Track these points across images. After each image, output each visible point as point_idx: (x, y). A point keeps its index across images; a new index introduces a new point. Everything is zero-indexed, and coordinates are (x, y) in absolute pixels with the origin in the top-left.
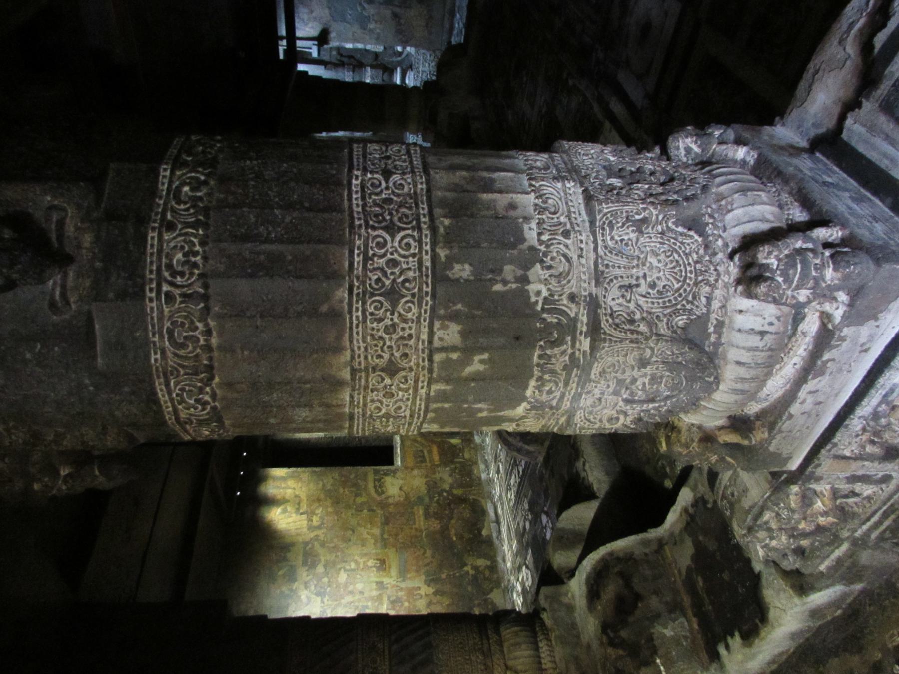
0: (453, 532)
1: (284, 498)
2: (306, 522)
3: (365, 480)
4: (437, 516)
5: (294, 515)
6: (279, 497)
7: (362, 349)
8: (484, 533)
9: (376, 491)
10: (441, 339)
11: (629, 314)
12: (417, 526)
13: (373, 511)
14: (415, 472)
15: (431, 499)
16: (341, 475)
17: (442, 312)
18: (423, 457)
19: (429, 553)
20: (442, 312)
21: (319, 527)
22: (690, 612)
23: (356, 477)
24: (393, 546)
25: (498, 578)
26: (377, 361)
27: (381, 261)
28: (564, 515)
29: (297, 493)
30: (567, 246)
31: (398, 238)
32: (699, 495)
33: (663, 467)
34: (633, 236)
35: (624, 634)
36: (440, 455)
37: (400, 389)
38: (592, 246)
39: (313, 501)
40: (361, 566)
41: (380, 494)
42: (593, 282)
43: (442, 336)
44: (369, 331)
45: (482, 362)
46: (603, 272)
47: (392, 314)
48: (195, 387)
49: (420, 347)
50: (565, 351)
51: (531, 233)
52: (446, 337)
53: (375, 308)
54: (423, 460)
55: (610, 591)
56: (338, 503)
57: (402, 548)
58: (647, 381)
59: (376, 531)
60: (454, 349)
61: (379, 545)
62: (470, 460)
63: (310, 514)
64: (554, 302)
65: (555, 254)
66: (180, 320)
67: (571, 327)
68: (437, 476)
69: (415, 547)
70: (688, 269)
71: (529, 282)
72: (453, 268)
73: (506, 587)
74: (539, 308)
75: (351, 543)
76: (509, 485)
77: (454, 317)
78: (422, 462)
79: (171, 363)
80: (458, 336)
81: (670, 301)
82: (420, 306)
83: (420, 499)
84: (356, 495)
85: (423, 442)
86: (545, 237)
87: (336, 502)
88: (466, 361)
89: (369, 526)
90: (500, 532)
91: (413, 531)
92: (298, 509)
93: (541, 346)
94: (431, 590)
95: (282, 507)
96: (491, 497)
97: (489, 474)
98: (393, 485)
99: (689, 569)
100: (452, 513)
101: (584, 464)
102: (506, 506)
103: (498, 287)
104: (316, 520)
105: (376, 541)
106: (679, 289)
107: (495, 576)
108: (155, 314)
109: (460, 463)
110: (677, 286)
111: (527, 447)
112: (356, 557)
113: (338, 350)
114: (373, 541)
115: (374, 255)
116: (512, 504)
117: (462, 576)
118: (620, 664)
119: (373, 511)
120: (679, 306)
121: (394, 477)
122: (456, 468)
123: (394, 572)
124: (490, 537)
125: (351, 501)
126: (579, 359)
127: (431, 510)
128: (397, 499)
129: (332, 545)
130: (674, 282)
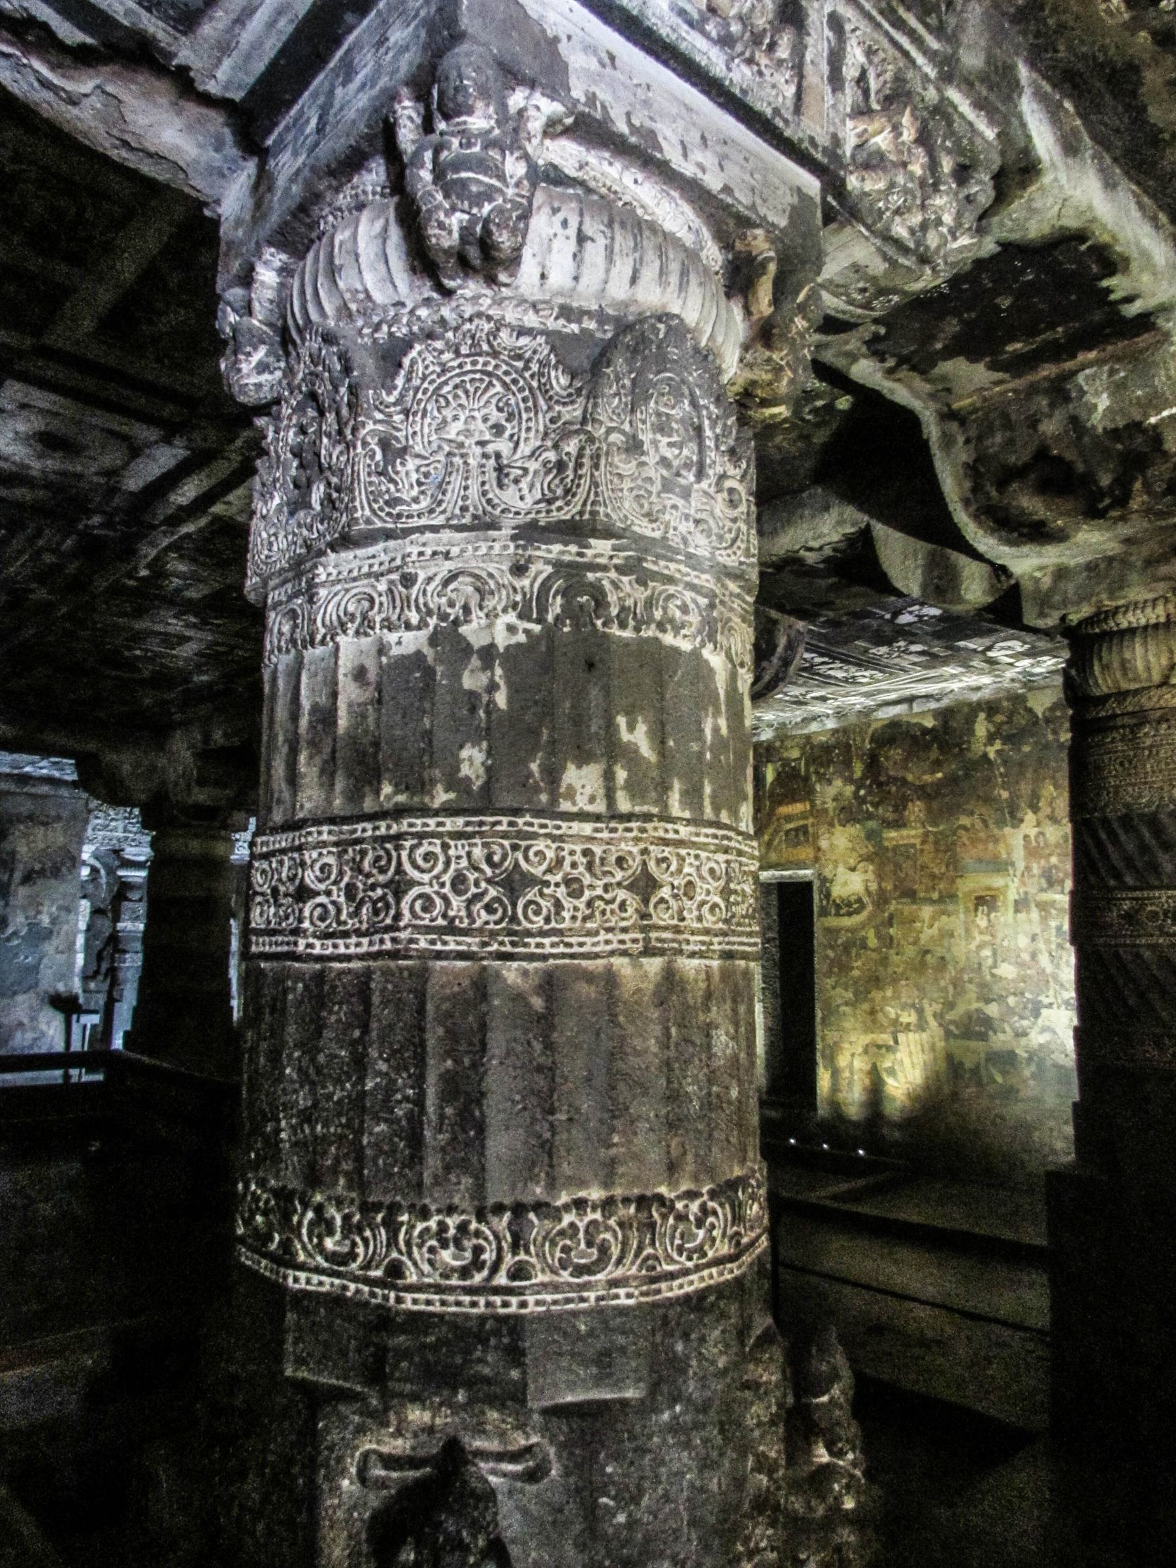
0: (927, 778)
4: (900, 805)
5: (899, 1055)
6: (867, 1082)
7: (610, 936)
8: (929, 723)
9: (857, 912)
10: (592, 799)
11: (549, 471)
12: (917, 841)
14: (824, 844)
15: (870, 816)
16: (829, 973)
17: (544, 798)
18: (797, 830)
19: (965, 821)
20: (544, 798)
21: (920, 1012)
22: (1069, 365)
23: (832, 947)
24: (953, 882)
26: (630, 910)
27: (455, 904)
28: (899, 585)
30: (430, 579)
31: (414, 874)
32: (864, 349)
33: (815, 411)
34: (411, 463)
35: (1105, 480)
36: (794, 800)
37: (679, 871)
38: (429, 536)
39: (874, 1021)
40: (987, 938)
41: (863, 906)
42: (493, 533)
43: (586, 798)
44: (578, 923)
45: (631, 728)
46: (475, 517)
47: (547, 884)
48: (675, 1228)
49: (605, 835)
50: (613, 582)
51: (407, 642)
52: (588, 790)
53: (537, 913)
54: (804, 830)
55: (1031, 504)
56: (877, 979)
57: (955, 867)
58: (665, 440)
59: (927, 911)
60: (609, 776)
61: (950, 908)
62: (803, 749)
63: (897, 1027)
64: (527, 602)
65: (444, 600)
66: (558, 1254)
67: (571, 575)
68: (830, 805)
70: (468, 367)
71: (492, 646)
72: (468, 778)
73: (1025, 685)
74: (537, 628)
75: (948, 957)
76: (846, 680)
77: (553, 775)
78: (806, 833)
79: (634, 1270)
80: (586, 770)
81: (524, 400)
82: (534, 836)
83: (871, 835)
84: (864, 946)
85: (770, 830)
86: (414, 618)
87: (876, 981)
88: (630, 755)
90: (928, 697)
92: (889, 1048)
93: (604, 624)
94: (1030, 817)
96: (867, 713)
99: (993, 367)
100: (896, 779)
101: (810, 549)
102: (882, 686)
103: (501, 699)
106: (504, 384)
108: (549, 1298)
110: (498, 388)
111: (780, 649)
112: (973, 947)
113: (610, 979)
114: (944, 918)
115: (445, 916)
116: (879, 675)
117: (1005, 763)
118: (1159, 488)
119: (891, 917)
120: (535, 384)
123: (998, 881)
124: (936, 714)
125: (874, 955)
126: (627, 558)
127: (890, 816)
128: (871, 876)
129: (951, 989)
130: (492, 391)
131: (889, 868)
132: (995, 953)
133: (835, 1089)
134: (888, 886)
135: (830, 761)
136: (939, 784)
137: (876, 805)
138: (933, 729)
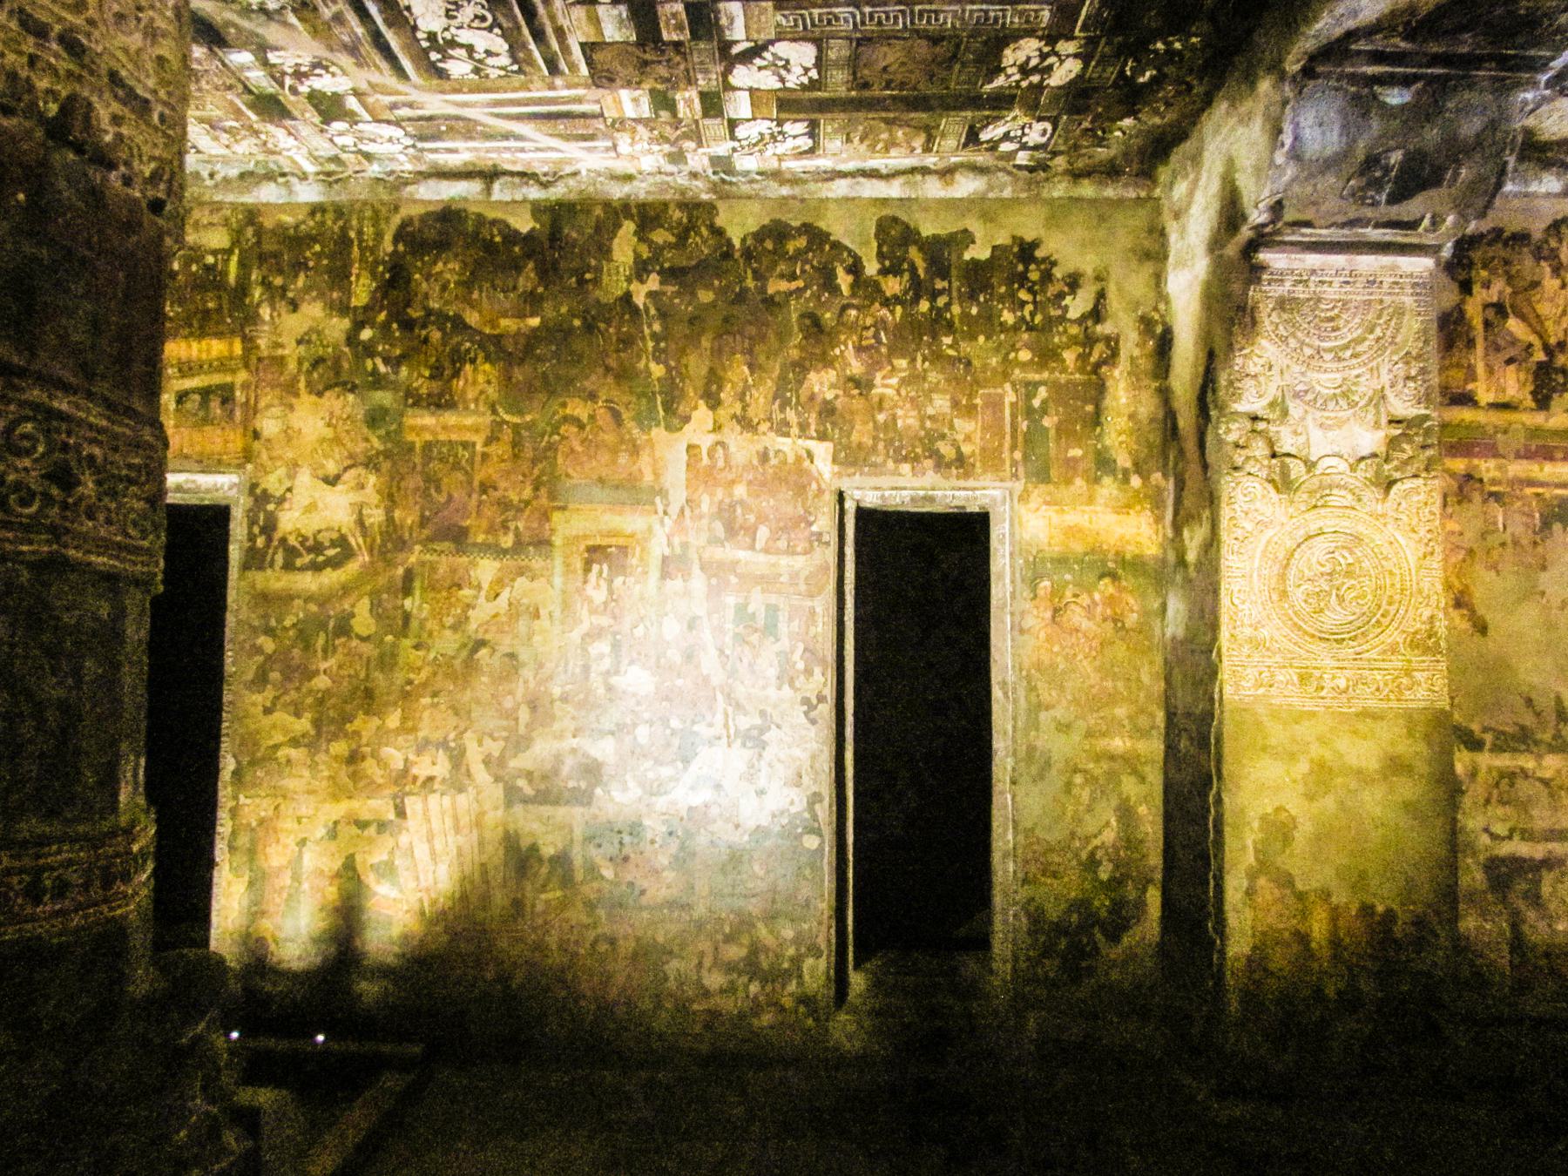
0: (508, 324)
1: (338, 875)
2: (433, 799)
3: (287, 598)
4: (448, 367)
5: (404, 839)
6: (332, 893)
8: (524, 223)
9: (335, 563)
12: (479, 440)
14: (269, 425)
15: (378, 382)
16: (261, 680)
18: (206, 393)
19: (579, 409)
21: (458, 759)
23: (269, 631)
24: (545, 516)
25: (682, 206)
29: (321, 832)
36: (202, 334)
39: (354, 776)
40: (604, 621)
41: (347, 553)
56: (369, 694)
57: (549, 489)
59: (486, 569)
61: (537, 563)
68: (291, 351)
69: (551, 447)
73: (714, 188)
75: (524, 656)
83: (375, 419)
84: (344, 628)
87: (368, 699)
89: (466, 592)
90: (525, 176)
91: (496, 450)
92: (382, 826)
95: (370, 879)
97: (304, 177)
98: (311, 508)
100: (441, 318)
104: (437, 765)
105: (521, 572)
107: (677, 214)
112: (576, 635)
114: (521, 582)
117: (663, 315)
119: (409, 576)
121: (281, 501)
122: (266, 284)
123: (631, 522)
124: (537, 209)
125: (367, 649)
127: (423, 385)
128: (371, 494)
129: (524, 714)
131: (414, 481)
132: (616, 646)
133: (256, 912)
134: (407, 517)
135: (299, 266)
136: (533, 339)
138: (530, 237)
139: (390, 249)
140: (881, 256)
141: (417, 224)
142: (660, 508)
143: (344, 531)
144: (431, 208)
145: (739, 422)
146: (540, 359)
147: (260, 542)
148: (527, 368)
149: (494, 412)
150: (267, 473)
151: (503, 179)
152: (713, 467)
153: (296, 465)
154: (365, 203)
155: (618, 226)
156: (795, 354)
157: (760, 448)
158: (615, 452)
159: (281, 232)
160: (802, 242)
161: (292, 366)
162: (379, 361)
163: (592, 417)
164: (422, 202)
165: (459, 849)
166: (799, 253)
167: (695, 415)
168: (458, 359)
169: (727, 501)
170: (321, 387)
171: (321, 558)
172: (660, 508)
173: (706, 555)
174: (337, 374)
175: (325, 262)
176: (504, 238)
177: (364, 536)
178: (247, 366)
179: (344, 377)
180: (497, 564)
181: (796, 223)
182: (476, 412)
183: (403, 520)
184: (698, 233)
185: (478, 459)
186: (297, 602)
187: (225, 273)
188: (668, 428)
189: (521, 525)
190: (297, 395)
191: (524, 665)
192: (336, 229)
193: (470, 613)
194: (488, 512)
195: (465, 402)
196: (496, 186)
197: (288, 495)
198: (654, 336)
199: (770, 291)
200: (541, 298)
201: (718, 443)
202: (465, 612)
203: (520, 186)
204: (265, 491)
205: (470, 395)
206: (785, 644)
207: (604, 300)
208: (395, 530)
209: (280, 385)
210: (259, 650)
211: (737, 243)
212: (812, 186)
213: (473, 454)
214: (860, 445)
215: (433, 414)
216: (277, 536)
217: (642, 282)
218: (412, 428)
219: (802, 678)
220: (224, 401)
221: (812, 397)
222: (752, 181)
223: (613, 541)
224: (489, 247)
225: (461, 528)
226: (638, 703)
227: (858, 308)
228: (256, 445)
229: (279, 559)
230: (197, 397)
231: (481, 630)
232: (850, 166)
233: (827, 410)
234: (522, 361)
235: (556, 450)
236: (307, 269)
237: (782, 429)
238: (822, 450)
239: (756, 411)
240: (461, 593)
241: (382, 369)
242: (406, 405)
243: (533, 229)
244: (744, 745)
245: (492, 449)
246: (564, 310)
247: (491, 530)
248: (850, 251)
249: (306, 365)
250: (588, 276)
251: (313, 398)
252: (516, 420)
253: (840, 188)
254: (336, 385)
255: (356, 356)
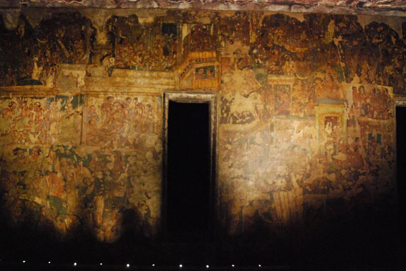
4: (280, 62)
8: (302, 20)
9: (248, 122)
12: (291, 84)
13: (272, 126)
14: (226, 79)
15: (259, 66)
18: (205, 68)
19: (320, 75)
36: (203, 50)
41: (252, 118)
69: (313, 87)
84: (253, 142)
85: (183, 67)
98: (241, 104)
100: (278, 47)
107: (346, 19)
109: (214, 29)
117: (343, 48)
119: (272, 126)
121: (231, 102)
124: (306, 15)
125: (259, 148)
134: (271, 107)
135: (233, 30)
137: (265, 60)
139: (261, 25)
140: (403, 33)
141: (269, 18)
142: (346, 106)
143: (251, 111)
144: (274, 13)
145: (367, 81)
146: (308, 60)
147: (225, 115)
148: (305, 62)
149: (295, 76)
150: (226, 93)
151: (294, 6)
152: (360, 93)
153: (235, 91)
154: (253, 11)
155: (329, 21)
156: (381, 61)
157: (373, 88)
158: (332, 88)
159: (226, 19)
160: (382, 28)
161: (232, 61)
162: (259, 59)
163: (325, 78)
164: (272, 11)
165: (290, 207)
166: (381, 31)
167: (355, 78)
168: (284, 59)
169: (365, 104)
170: (242, 67)
171: (244, 120)
172: (346, 106)
173: (360, 120)
174: (247, 63)
175: (241, 29)
176: (296, 24)
177: (257, 113)
178: (218, 61)
179: (248, 65)
180: (299, 122)
181: (380, 23)
182: (290, 76)
183: (269, 109)
184: (353, 24)
185: (291, 90)
186: (238, 134)
187: (209, 31)
188: (347, 82)
189: (306, 110)
190: (234, 70)
191: (308, 152)
192: (244, 19)
193: (292, 137)
194: (295, 106)
195: (286, 73)
196: (293, 7)
197: (233, 101)
198: (341, 54)
199: (373, 42)
200: (307, 42)
201: (361, 86)
202: (290, 136)
203: (300, 7)
204: (226, 99)
205: (288, 71)
206: (383, 145)
207: (327, 43)
208: (267, 112)
209: (229, 66)
210: (226, 149)
211: (363, 27)
212: (383, 12)
213: (290, 88)
214: (400, 88)
215: (277, 76)
216: (230, 113)
217: (337, 38)
218: (270, 81)
219: (388, 155)
220: (211, 71)
221: (387, 74)
222: (367, 10)
223: (333, 115)
224: (292, 26)
225: (287, 111)
226: (342, 163)
227: (397, 48)
228: (222, 85)
229: (231, 121)
230: (203, 70)
231: (295, 142)
232: (395, 7)
233: (391, 78)
234: (303, 61)
235: (315, 88)
236: (236, 31)
237: (379, 83)
238: (390, 89)
239: (371, 78)
240: (288, 131)
241: (260, 62)
242: (268, 73)
243: (304, 21)
244: (372, 175)
245: (294, 87)
246: (315, 45)
247: (296, 112)
248: (395, 31)
249: (237, 61)
250: (321, 36)
251: (240, 71)
252: (302, 78)
253: (391, 13)
254: (246, 67)
255: (252, 58)
